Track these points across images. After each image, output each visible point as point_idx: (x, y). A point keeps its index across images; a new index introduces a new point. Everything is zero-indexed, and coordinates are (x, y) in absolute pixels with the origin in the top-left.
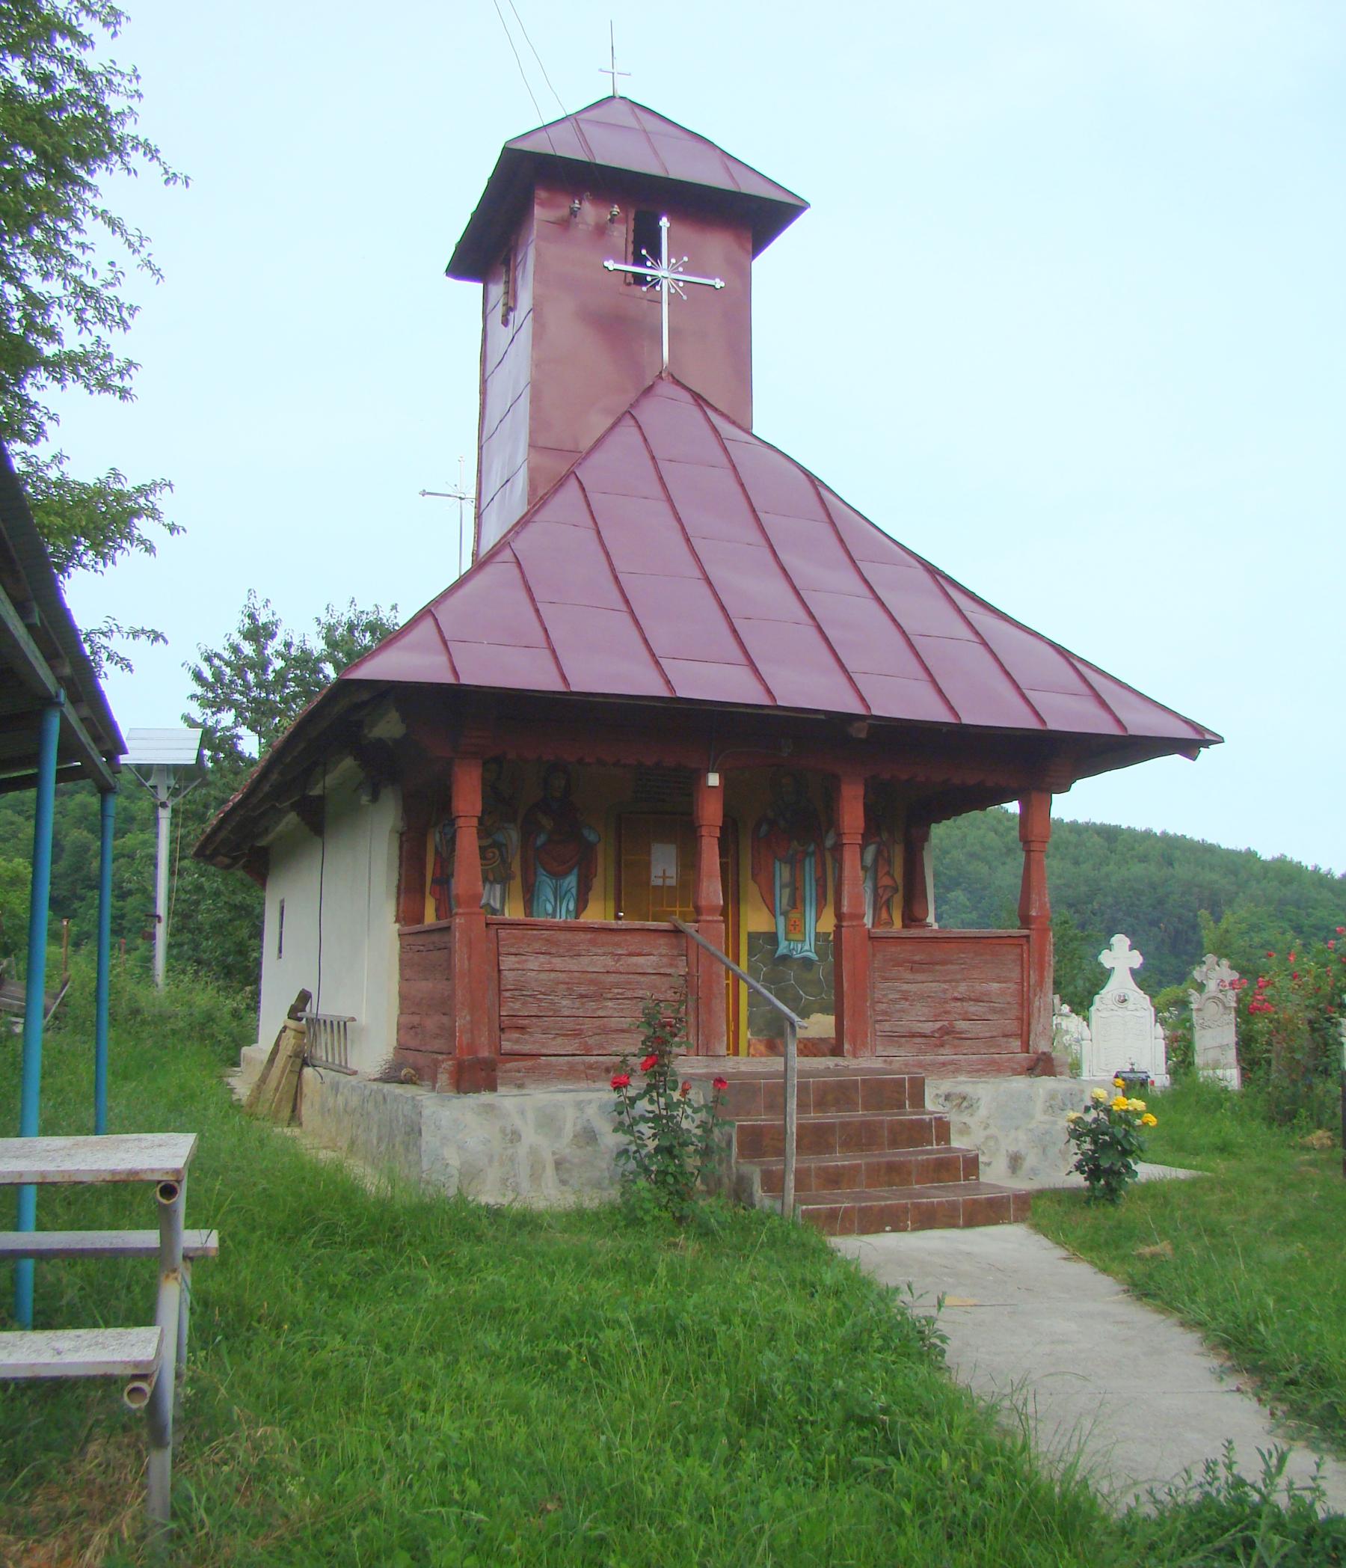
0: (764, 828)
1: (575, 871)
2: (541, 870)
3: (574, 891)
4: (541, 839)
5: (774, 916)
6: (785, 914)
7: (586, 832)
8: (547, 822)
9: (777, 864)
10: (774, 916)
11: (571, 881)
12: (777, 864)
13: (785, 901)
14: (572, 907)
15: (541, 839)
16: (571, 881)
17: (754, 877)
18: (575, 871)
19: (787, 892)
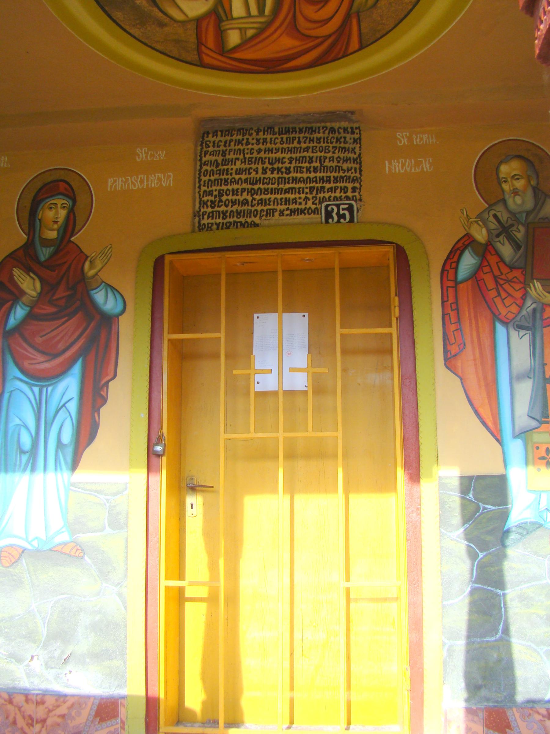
0: (468, 262)
1: (77, 369)
2: (13, 371)
3: (73, 407)
4: (19, 313)
5: (499, 440)
6: (523, 434)
7: (99, 296)
8: (30, 285)
9: (501, 330)
10: (499, 440)
11: (69, 387)
12: (501, 330)
13: (523, 405)
14: (67, 436)
15: (19, 313)
16: (69, 387)
17: (450, 361)
18: (77, 369)
19: (525, 390)
